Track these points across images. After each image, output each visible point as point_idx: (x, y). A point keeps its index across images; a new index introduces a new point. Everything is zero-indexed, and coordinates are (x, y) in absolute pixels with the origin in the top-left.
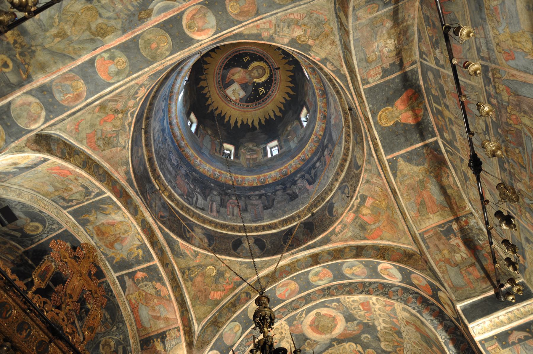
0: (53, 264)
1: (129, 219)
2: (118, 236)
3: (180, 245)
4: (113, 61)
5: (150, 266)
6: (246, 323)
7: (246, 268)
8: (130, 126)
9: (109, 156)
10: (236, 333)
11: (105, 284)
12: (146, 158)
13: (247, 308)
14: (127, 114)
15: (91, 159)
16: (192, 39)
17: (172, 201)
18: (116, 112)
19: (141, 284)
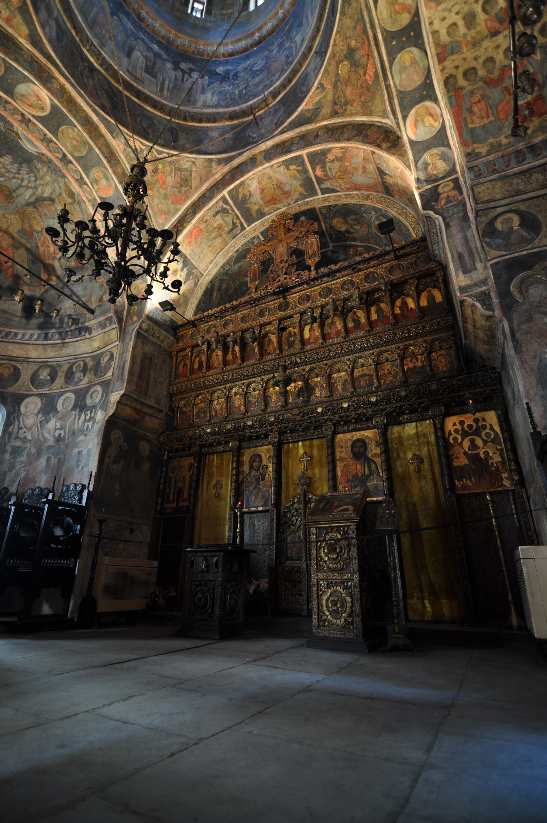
3: (306, 108)
5: (309, 160)
6: (409, 37)
7: (350, 4)
9: (199, 181)
10: (414, 62)
12: (227, 123)
13: (384, 31)
16: (52, 105)
17: (279, 93)
18: (155, 171)
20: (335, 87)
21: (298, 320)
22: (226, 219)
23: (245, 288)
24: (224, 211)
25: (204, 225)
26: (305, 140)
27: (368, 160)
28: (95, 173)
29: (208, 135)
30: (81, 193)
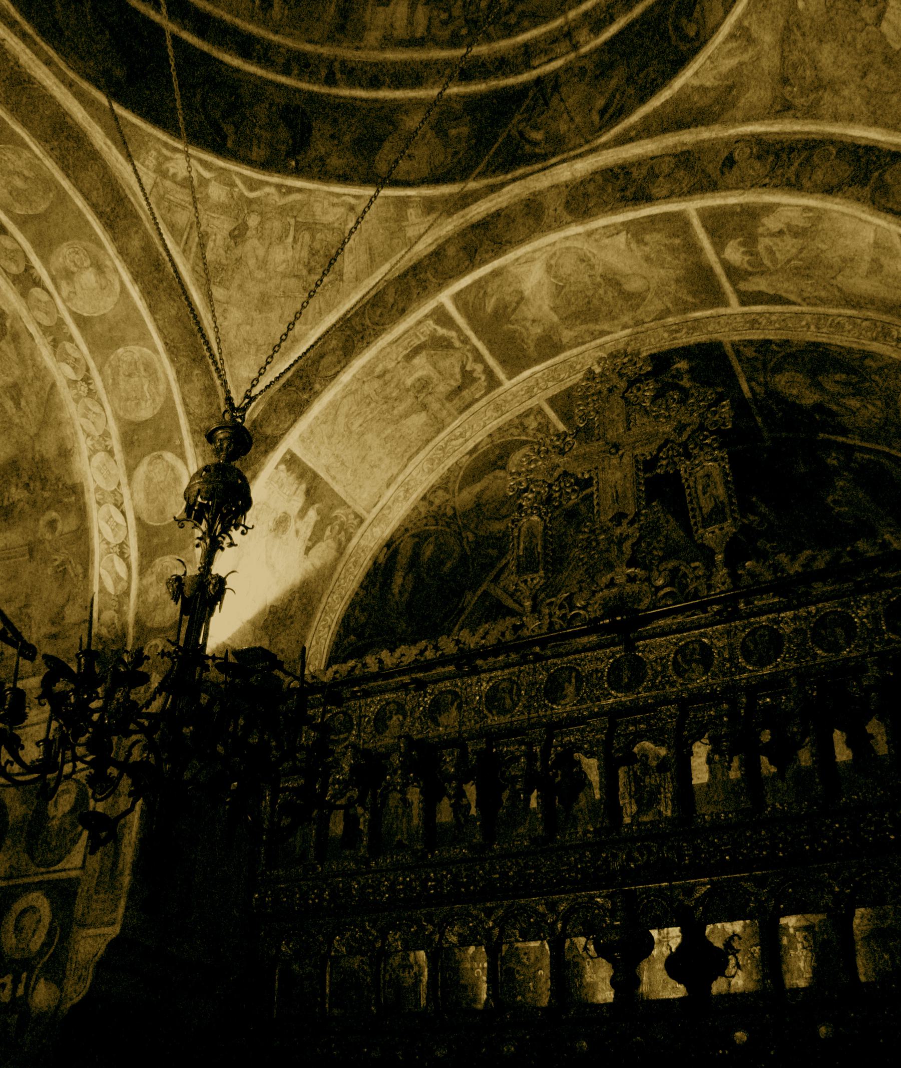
0: (535, 518)
1: (540, 249)
2: (599, 279)
4: (73, 273)
5: (704, 226)
8: (290, 190)
9: (364, 258)
11: (742, 348)
14: (250, 202)
15: (356, 314)
17: (612, 20)
18: (238, 235)
19: (766, 262)
20: (785, 40)
21: (672, 724)
22: (445, 364)
23: (494, 552)
24: (440, 345)
25: (376, 384)
26: (695, 171)
27: (889, 249)
28: (64, 255)
29: (395, 125)
30: (24, 313)
